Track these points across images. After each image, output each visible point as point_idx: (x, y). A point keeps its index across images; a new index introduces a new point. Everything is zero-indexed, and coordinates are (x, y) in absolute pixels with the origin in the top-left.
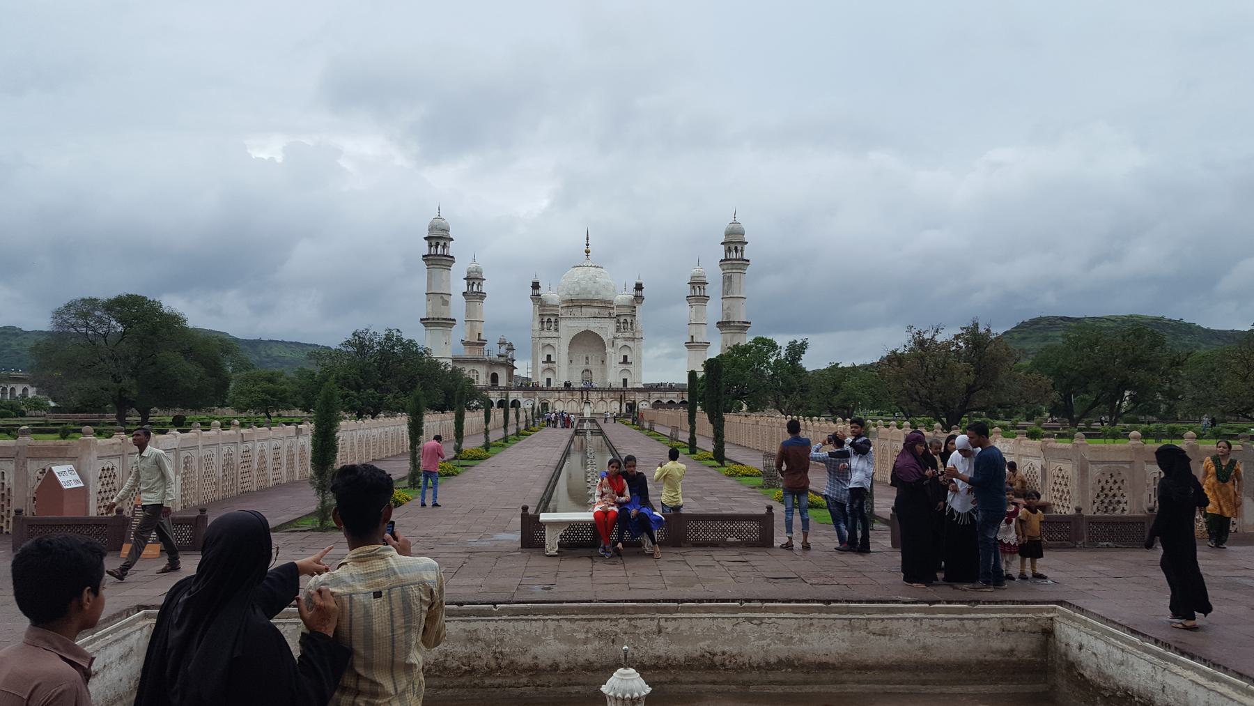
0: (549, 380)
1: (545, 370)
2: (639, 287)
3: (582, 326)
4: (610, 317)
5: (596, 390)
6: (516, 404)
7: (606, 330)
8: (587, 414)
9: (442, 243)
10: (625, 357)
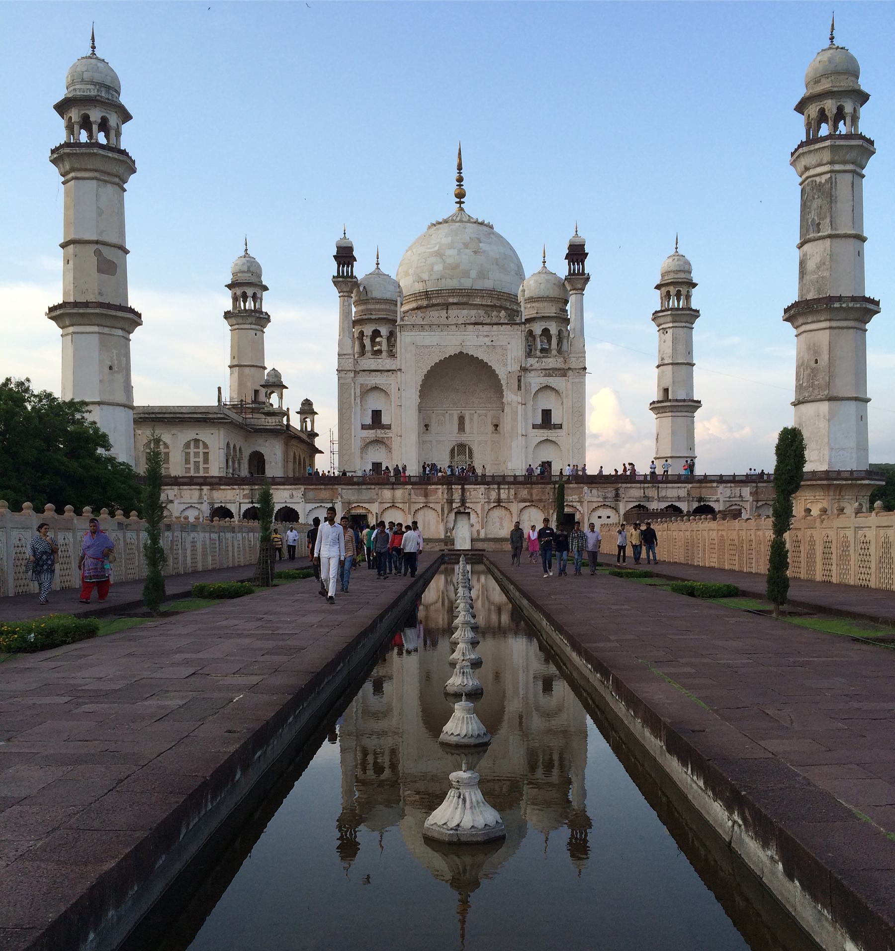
0: (377, 466)
2: (577, 254)
4: (511, 323)
5: (484, 480)
7: (503, 349)
8: (463, 542)
10: (547, 414)
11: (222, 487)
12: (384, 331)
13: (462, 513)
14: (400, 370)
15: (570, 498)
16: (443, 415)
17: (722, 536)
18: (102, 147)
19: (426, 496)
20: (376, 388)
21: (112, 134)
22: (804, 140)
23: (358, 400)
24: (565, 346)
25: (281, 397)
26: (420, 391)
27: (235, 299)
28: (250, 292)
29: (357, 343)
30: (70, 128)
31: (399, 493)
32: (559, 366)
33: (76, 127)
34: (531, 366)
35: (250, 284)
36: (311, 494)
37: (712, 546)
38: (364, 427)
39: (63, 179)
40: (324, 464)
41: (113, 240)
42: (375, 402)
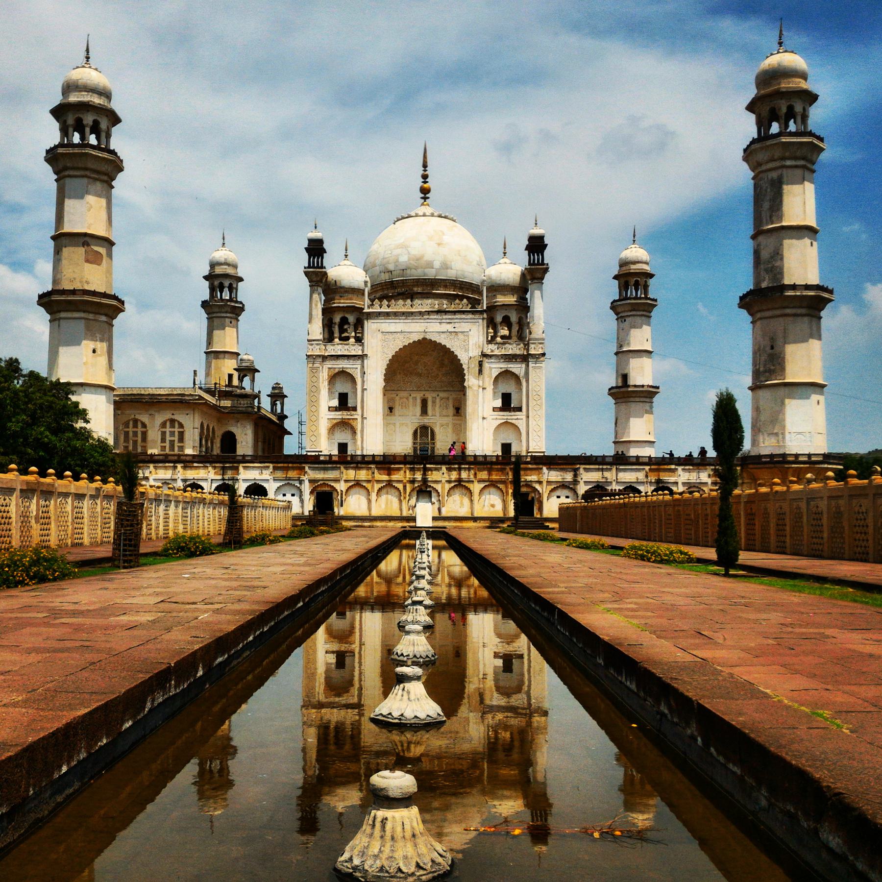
0: (343, 447)
1: (335, 427)
3: (412, 330)
11: (195, 465)
12: (351, 319)
13: (424, 491)
14: (366, 355)
15: (529, 478)
16: (407, 398)
17: (679, 511)
18: (93, 147)
19: (389, 474)
21: (103, 135)
22: (756, 136)
23: (326, 383)
24: (523, 335)
25: (253, 380)
26: (385, 375)
27: (212, 289)
28: (226, 283)
29: (326, 330)
30: (65, 131)
32: (518, 352)
33: (71, 130)
34: (492, 351)
35: (226, 276)
36: (279, 474)
37: (669, 522)
38: (330, 409)
39: (56, 177)
40: (290, 446)
41: (101, 231)
42: (342, 387)
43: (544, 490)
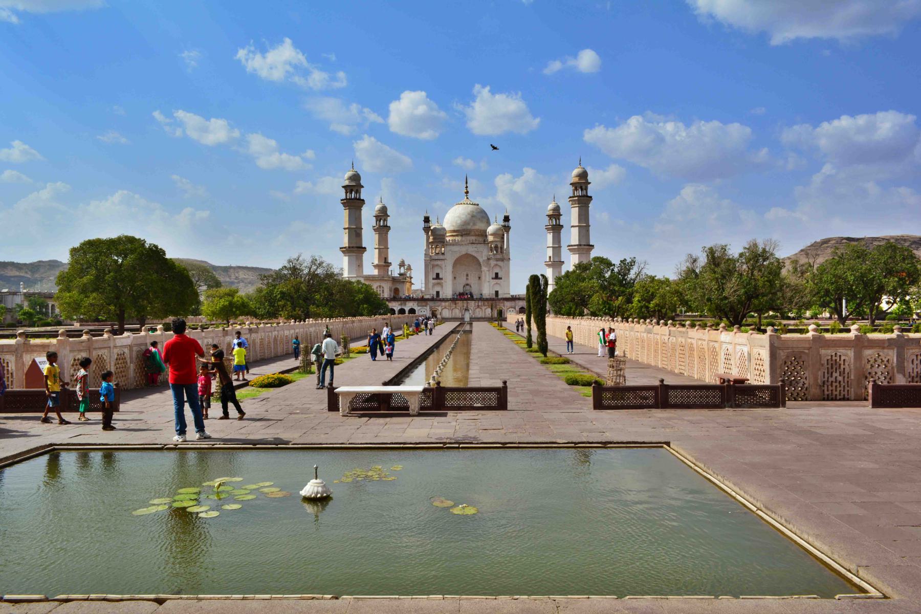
0: (438, 293)
1: (434, 285)
6: (412, 311)
7: (482, 253)
9: (355, 189)
10: (497, 274)
20: (437, 265)
31: (447, 304)
43: (504, 309)
